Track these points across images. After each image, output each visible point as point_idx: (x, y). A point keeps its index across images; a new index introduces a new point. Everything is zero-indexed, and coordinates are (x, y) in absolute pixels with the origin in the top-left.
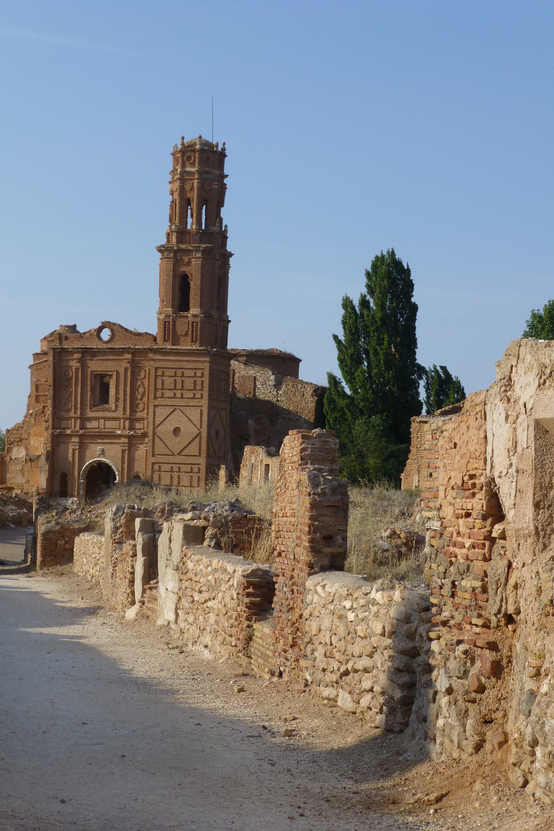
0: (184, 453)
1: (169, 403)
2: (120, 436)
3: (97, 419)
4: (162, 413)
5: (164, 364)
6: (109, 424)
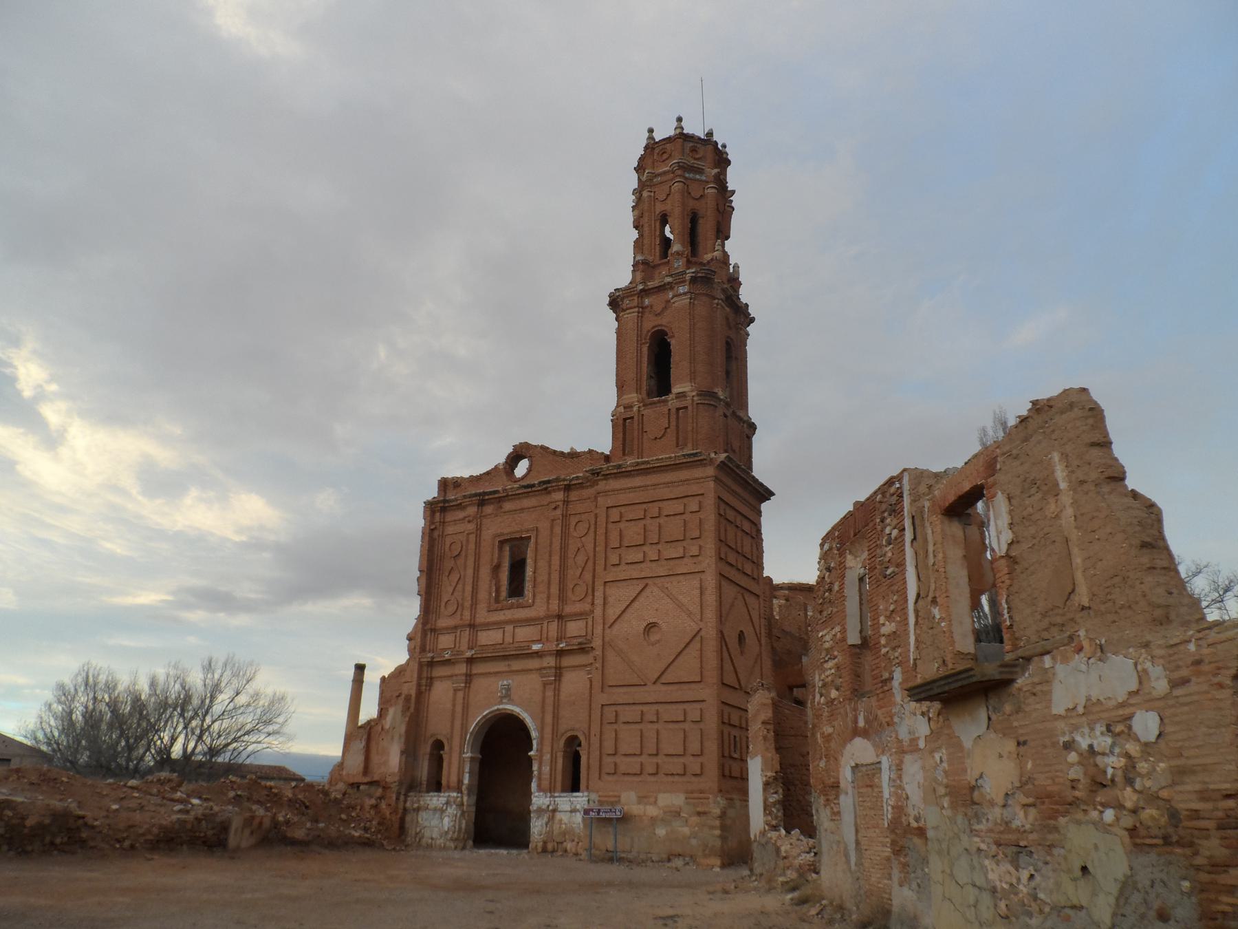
0: (668, 677)
1: (635, 575)
2: (538, 654)
3: (499, 625)
4: (619, 596)
5: (624, 498)
6: (523, 633)
